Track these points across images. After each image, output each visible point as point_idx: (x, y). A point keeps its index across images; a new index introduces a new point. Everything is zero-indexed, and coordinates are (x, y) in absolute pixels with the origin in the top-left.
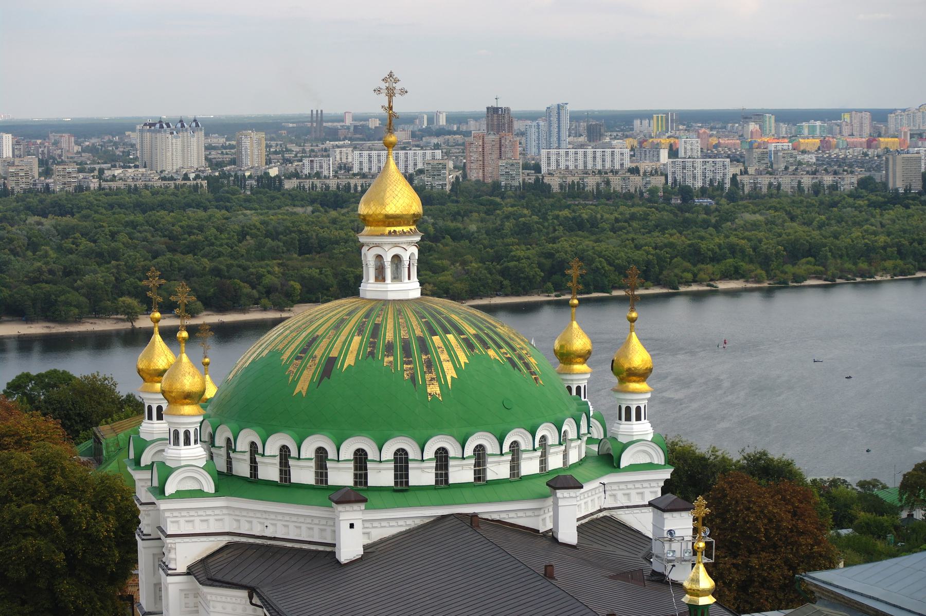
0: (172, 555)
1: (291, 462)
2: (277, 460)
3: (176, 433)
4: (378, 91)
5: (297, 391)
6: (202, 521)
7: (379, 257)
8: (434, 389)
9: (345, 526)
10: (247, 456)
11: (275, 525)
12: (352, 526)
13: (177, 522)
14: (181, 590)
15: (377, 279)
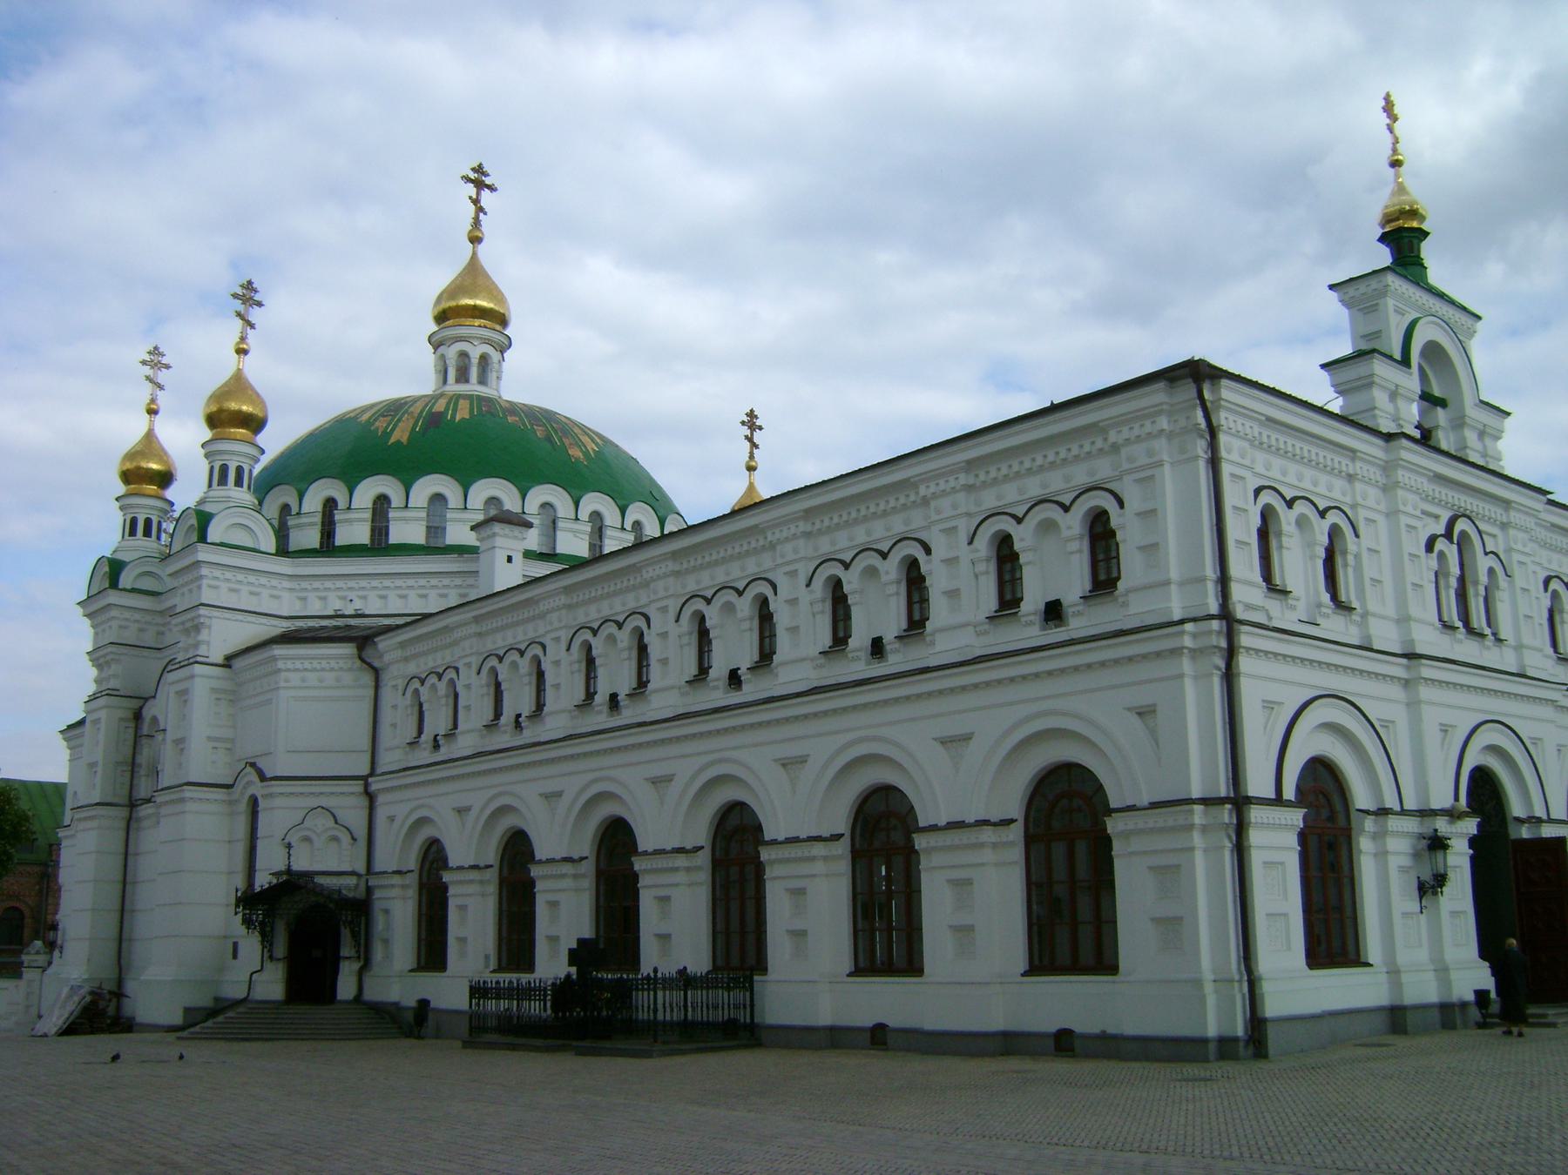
0: (204, 635)
1: (391, 515)
2: (368, 515)
3: (224, 469)
4: (467, 179)
5: (392, 440)
6: (251, 593)
7: (464, 355)
8: (575, 452)
9: (501, 557)
10: (318, 519)
11: (364, 598)
12: (510, 559)
13: (216, 587)
14: (213, 690)
15: (458, 381)
